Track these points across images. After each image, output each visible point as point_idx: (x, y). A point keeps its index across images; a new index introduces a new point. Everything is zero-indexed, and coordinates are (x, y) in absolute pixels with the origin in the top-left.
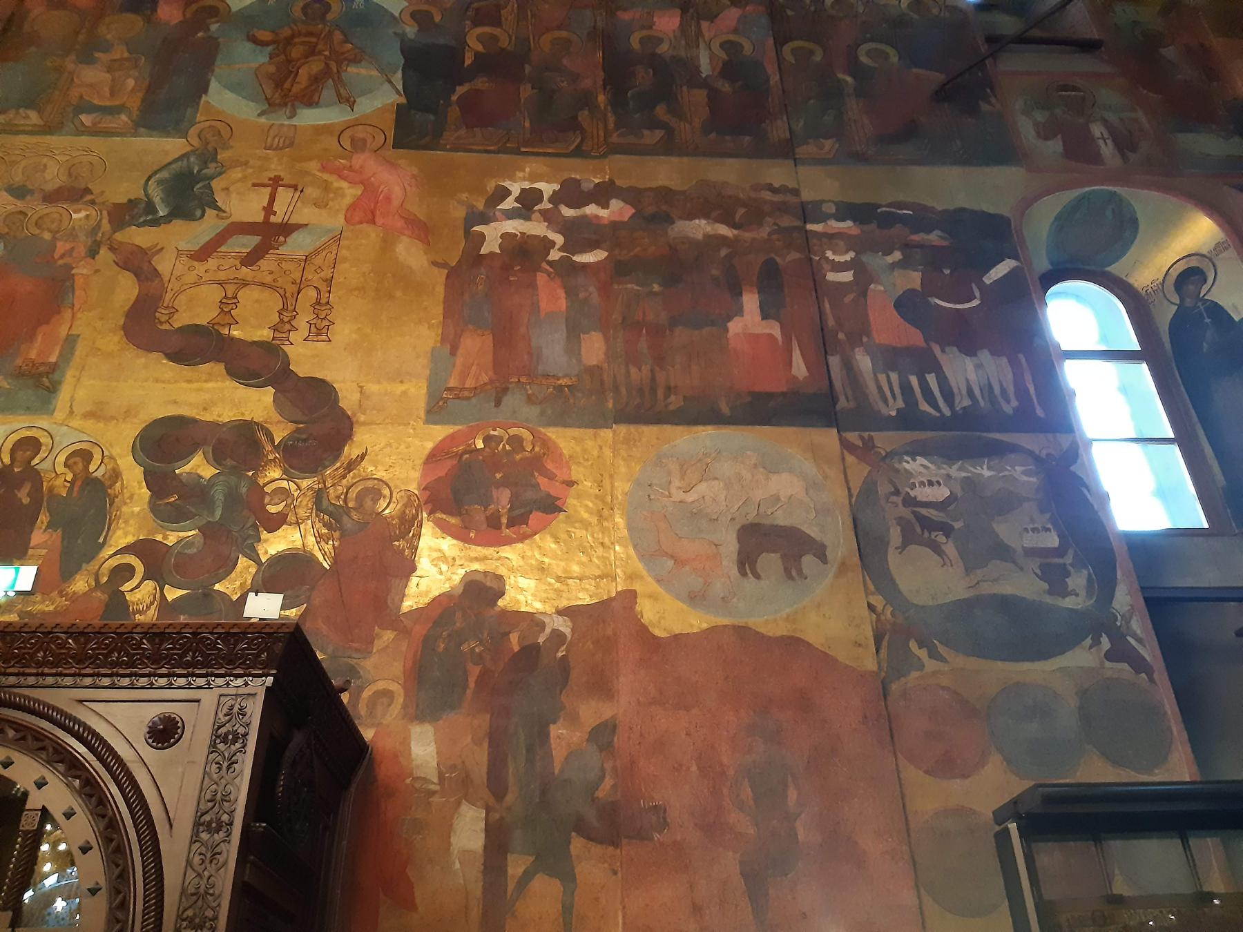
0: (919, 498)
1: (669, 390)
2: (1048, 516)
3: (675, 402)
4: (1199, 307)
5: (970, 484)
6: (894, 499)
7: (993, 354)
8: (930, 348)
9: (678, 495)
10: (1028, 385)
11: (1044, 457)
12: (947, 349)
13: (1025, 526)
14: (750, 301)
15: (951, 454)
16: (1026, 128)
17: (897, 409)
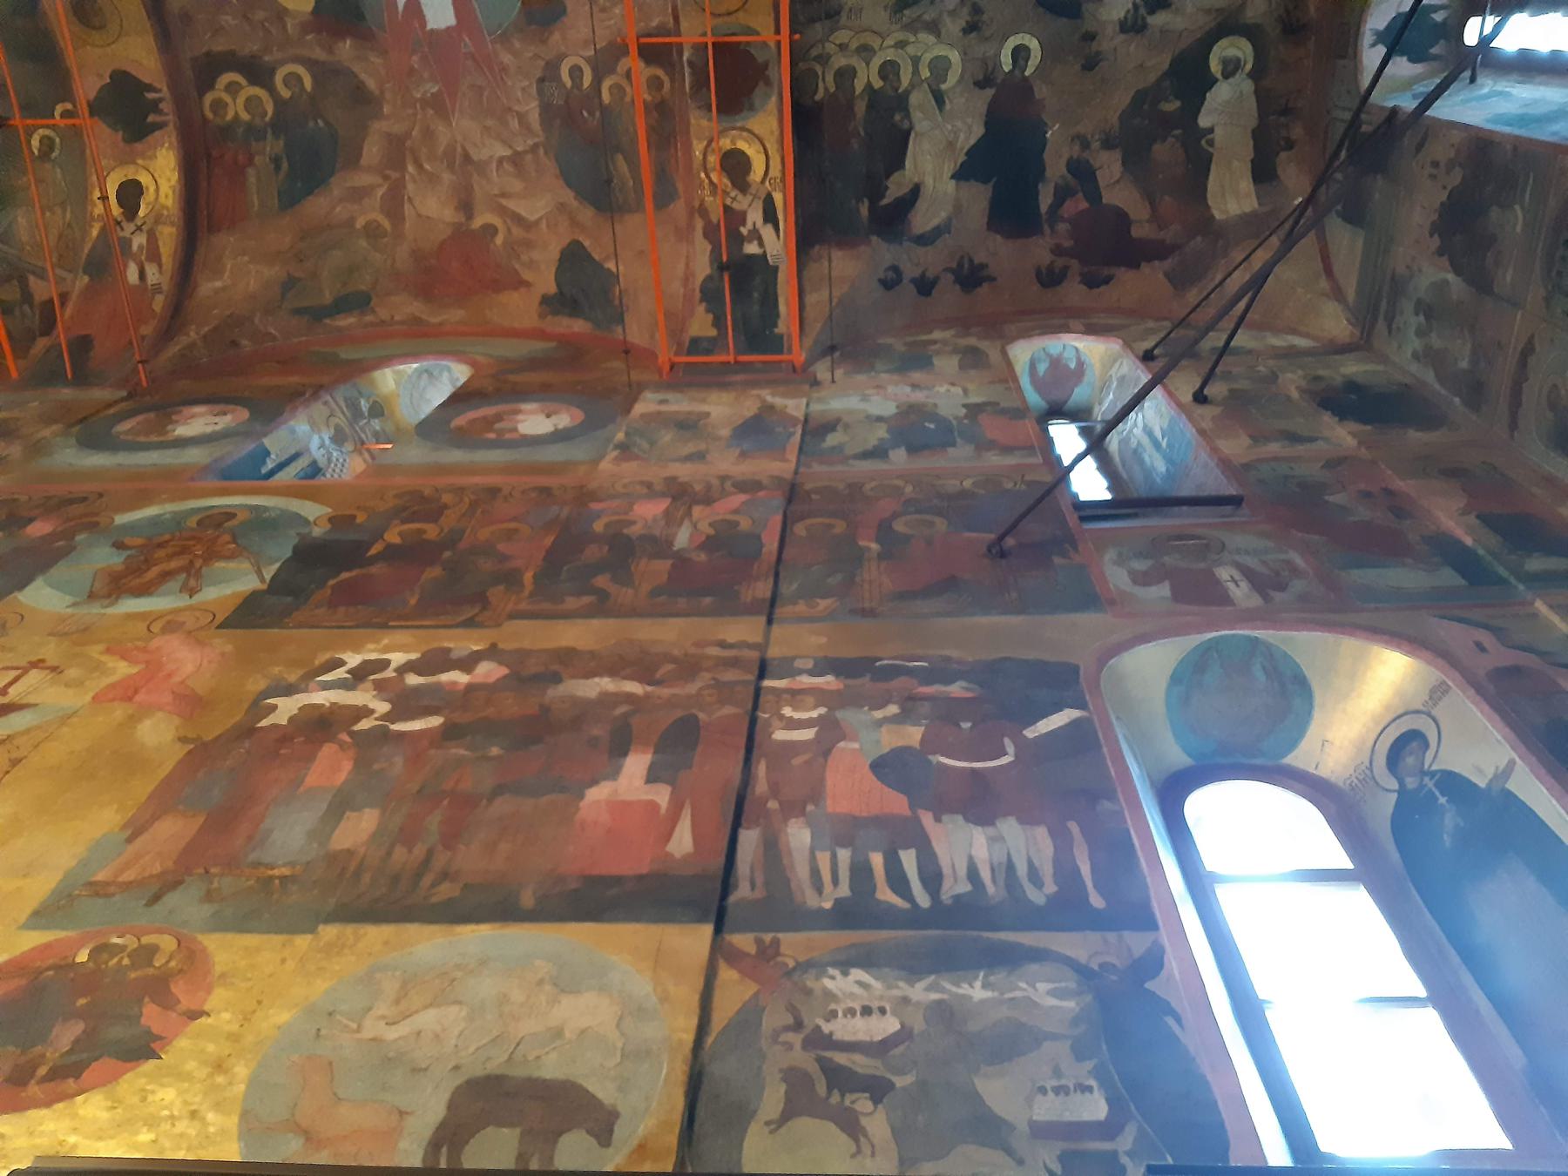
0: (838, 1036)
1: (445, 876)
2: (1089, 1065)
3: (446, 891)
4: (1426, 785)
5: (945, 1014)
6: (790, 1037)
7: (1021, 821)
8: (917, 820)
9: (372, 1028)
10: (1079, 863)
11: (1096, 968)
12: (945, 818)
13: (1041, 1083)
14: (636, 764)
15: (914, 965)
16: (1117, 577)
17: (836, 900)
